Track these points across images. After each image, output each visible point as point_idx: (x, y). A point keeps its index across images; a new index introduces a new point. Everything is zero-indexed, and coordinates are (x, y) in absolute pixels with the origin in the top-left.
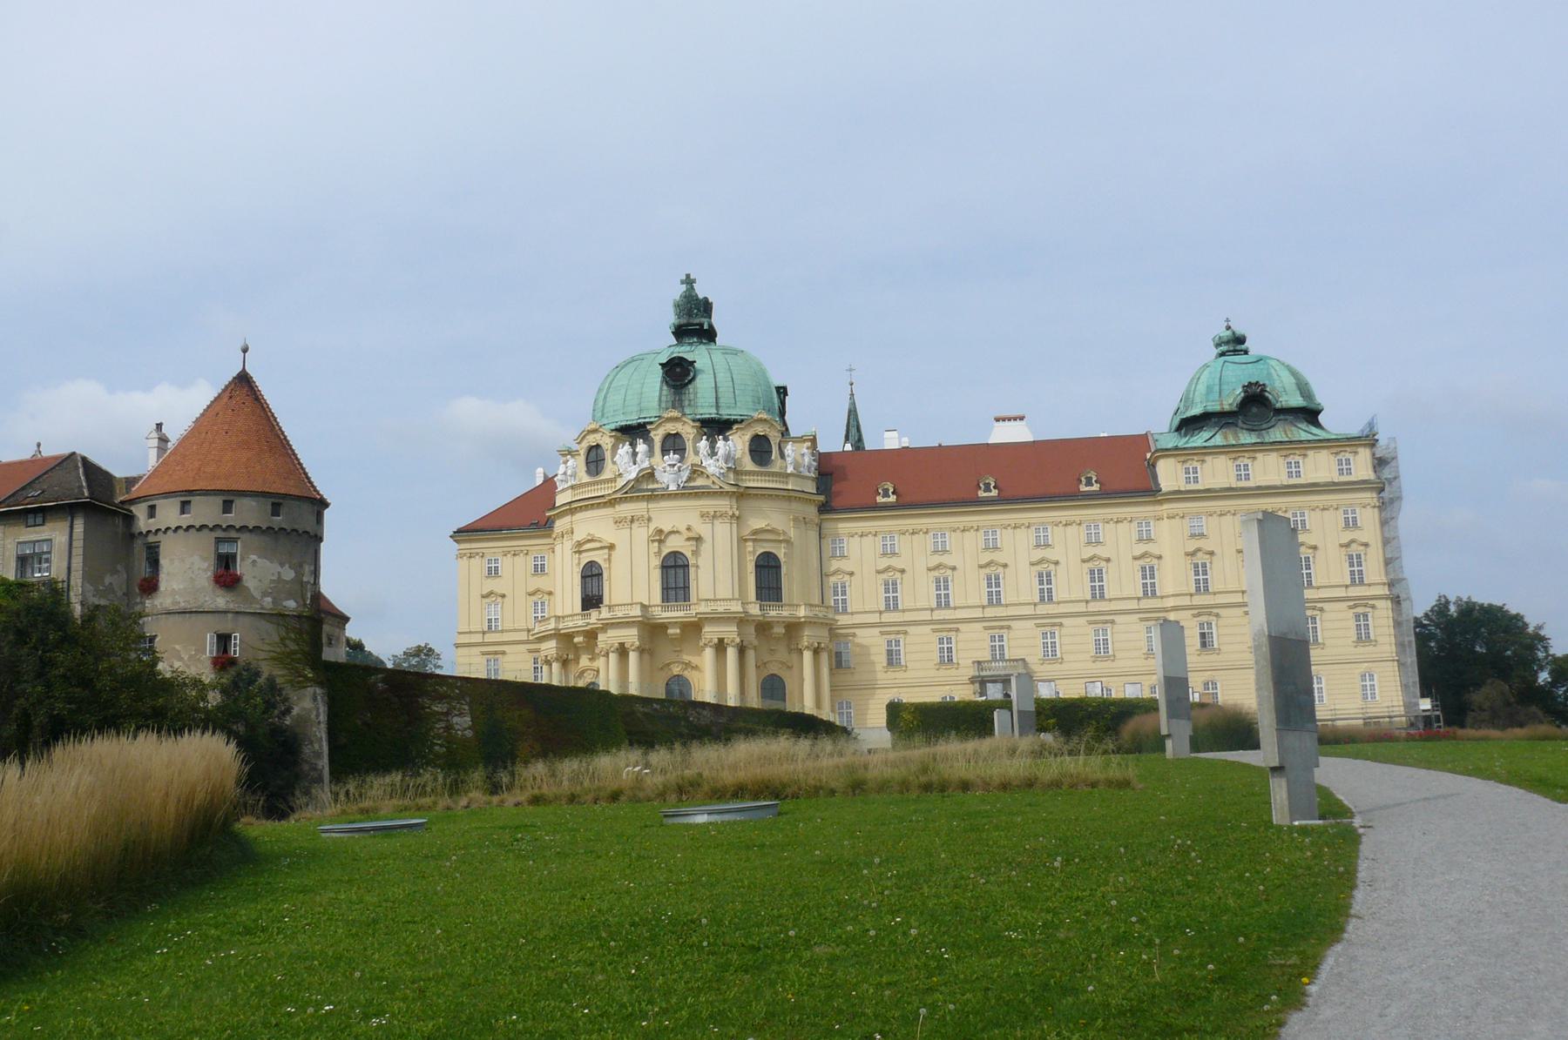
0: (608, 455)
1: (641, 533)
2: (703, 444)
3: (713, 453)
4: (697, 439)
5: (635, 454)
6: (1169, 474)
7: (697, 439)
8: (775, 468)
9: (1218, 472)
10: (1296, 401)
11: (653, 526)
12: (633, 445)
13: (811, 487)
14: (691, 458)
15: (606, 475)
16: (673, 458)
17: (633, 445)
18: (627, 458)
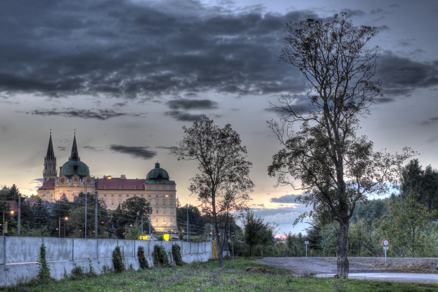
0: (65, 180)
1: (71, 193)
2: (80, 180)
3: (82, 182)
4: (79, 179)
5: (70, 181)
6: (146, 187)
7: (79, 179)
8: (90, 184)
9: (154, 187)
10: (166, 177)
11: (73, 192)
12: (70, 179)
13: (94, 186)
14: (79, 182)
15: (65, 183)
16: (76, 182)
17: (70, 179)
18: (69, 182)
